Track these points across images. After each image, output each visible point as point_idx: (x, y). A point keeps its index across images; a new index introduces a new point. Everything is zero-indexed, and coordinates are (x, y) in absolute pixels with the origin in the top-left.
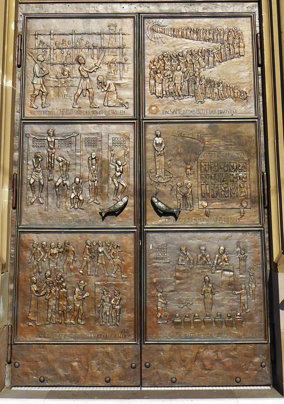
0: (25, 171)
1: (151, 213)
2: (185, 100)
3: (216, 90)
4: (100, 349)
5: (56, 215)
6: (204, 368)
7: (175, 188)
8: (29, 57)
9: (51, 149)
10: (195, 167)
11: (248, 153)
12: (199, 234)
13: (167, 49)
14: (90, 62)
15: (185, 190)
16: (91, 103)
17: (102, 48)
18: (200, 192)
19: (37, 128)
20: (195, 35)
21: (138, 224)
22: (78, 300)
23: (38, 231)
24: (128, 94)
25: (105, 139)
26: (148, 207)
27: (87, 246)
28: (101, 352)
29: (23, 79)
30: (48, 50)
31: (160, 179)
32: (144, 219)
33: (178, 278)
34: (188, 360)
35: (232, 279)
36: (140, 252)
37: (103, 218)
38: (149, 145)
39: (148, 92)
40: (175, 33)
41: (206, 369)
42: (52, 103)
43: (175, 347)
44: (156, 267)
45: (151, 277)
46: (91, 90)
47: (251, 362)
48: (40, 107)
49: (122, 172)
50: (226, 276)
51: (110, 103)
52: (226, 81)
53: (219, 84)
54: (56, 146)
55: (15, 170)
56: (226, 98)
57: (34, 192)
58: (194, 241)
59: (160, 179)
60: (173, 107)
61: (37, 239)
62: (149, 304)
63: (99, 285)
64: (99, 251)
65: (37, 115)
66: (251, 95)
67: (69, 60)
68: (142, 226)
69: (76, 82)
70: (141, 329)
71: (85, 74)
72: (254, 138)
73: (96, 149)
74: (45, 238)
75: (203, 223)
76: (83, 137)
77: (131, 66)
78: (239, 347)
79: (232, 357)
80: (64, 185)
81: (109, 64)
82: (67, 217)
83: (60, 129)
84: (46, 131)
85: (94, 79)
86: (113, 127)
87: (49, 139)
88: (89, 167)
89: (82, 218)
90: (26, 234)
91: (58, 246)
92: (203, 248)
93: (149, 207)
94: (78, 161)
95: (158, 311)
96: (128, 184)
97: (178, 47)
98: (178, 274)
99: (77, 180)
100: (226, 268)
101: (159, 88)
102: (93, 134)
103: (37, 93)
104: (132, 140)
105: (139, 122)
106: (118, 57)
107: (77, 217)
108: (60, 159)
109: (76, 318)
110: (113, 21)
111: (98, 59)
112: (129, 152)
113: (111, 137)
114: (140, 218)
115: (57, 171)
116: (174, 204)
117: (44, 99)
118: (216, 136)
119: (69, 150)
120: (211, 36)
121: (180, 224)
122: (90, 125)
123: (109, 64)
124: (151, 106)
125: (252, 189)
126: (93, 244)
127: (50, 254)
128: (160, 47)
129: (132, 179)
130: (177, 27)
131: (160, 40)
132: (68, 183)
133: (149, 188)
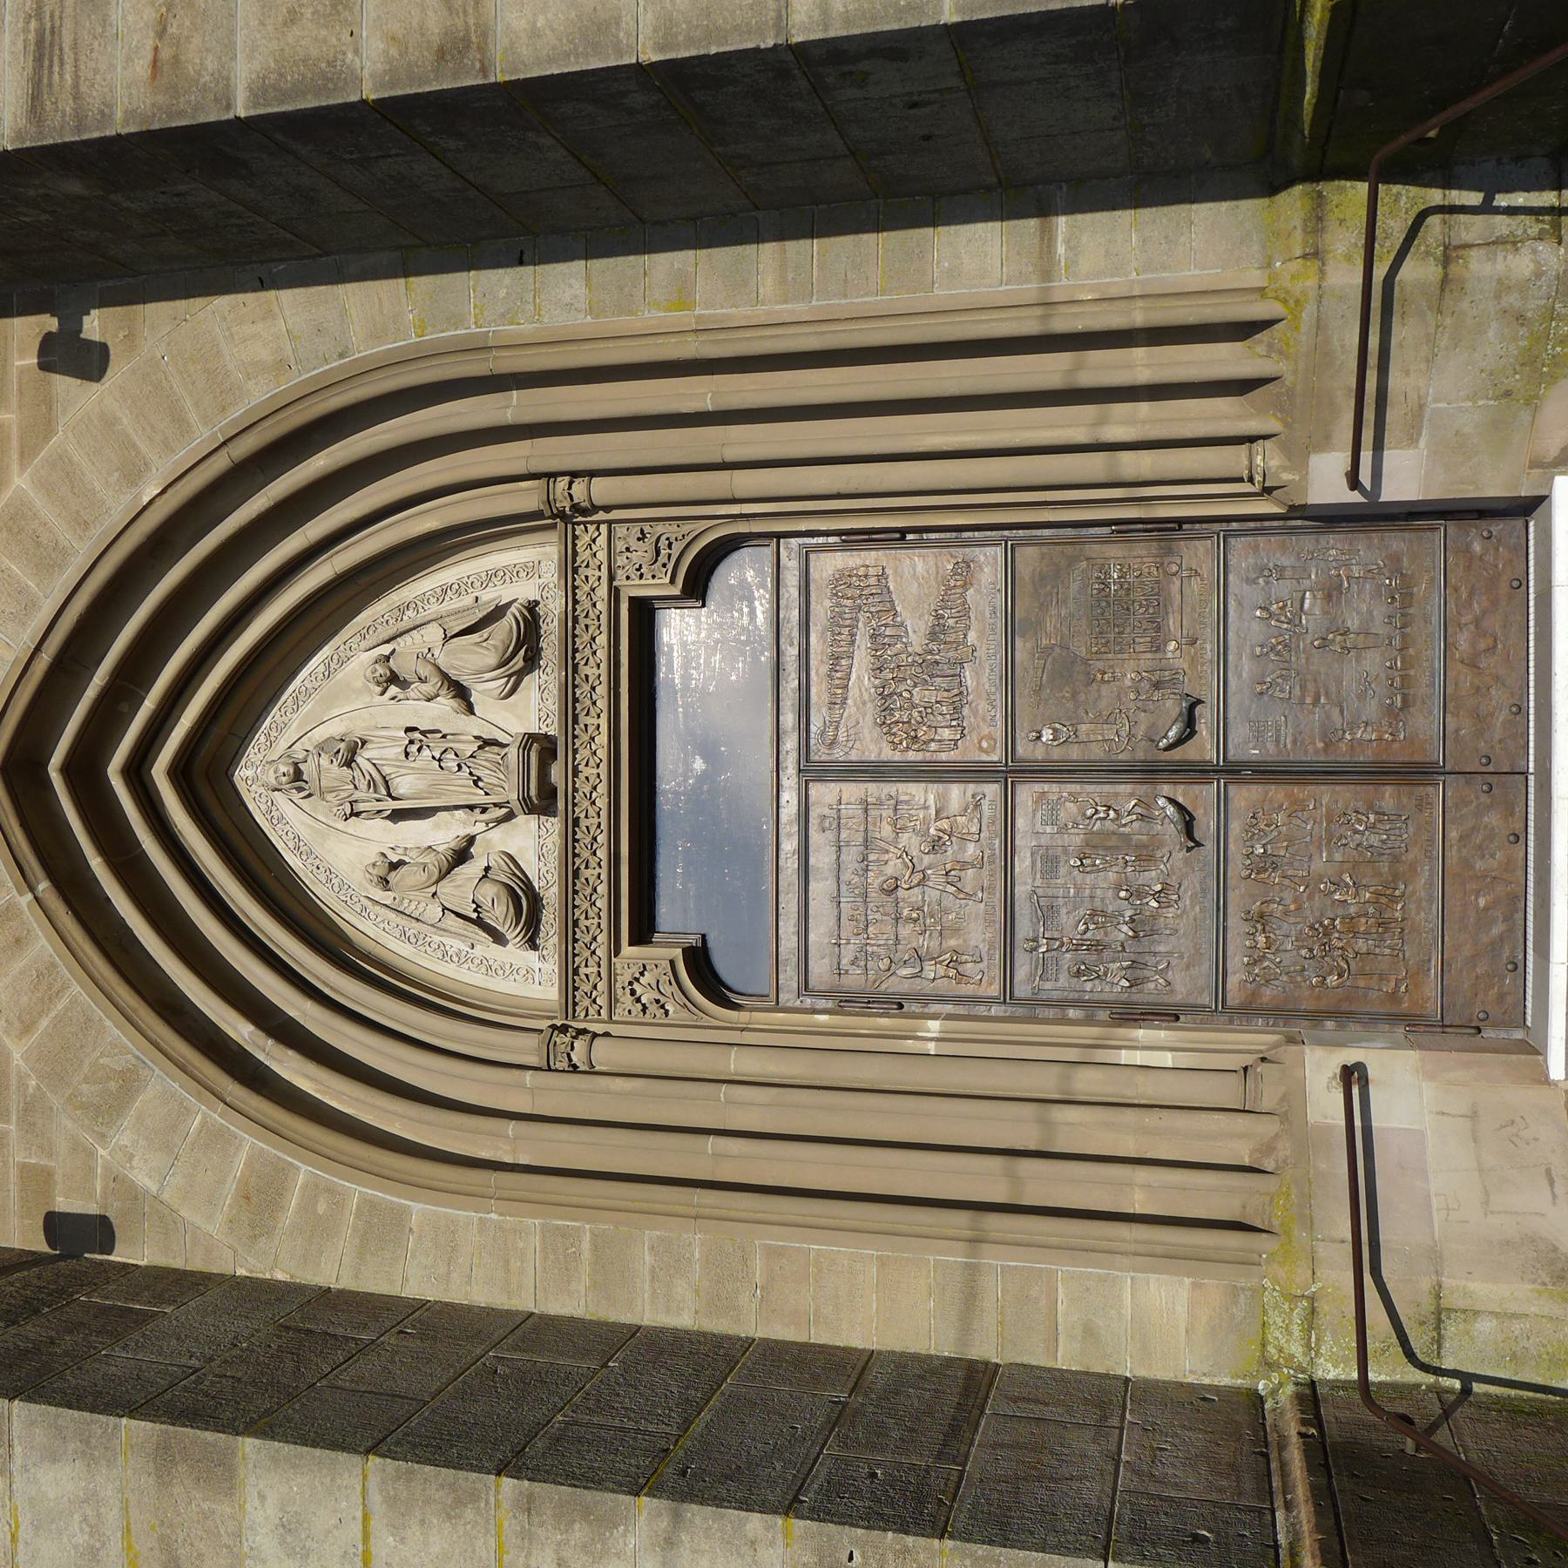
0: (1105, 997)
1: (1189, 752)
2: (969, 683)
3: (951, 622)
4: (1453, 854)
6: (1491, 649)
7: (1140, 704)
8: (883, 987)
9: (1062, 945)
10: (1100, 665)
12: (1230, 658)
13: (869, 718)
14: (893, 867)
15: (1145, 685)
16: (974, 866)
17: (866, 843)
18: (1149, 656)
19: (1021, 973)
20: (843, 662)
22: (1357, 894)
24: (957, 794)
25: (1044, 841)
26: (1177, 758)
28: (1459, 850)
29: (924, 999)
30: (870, 949)
31: (1123, 734)
33: (1317, 700)
34: (1476, 681)
35: (1319, 595)
36: (1265, 772)
37: (1198, 844)
38: (1056, 754)
39: (953, 755)
40: (837, 702)
41: (1495, 647)
42: (972, 943)
43: (1450, 706)
44: (1294, 742)
45: (1313, 752)
46: (948, 867)
47: (1481, 558)
48: (981, 966)
49: (1109, 808)
50: (1312, 605)
51: (974, 829)
52: (933, 602)
53: (938, 617)
55: (1103, 1015)
56: (965, 602)
57: (1146, 980)
58: (1243, 669)
59: (1123, 734)
60: (983, 706)
62: (1366, 756)
63: (1329, 854)
65: (997, 972)
66: (960, 553)
67: (890, 909)
69: (932, 895)
70: (1416, 773)
71: (917, 878)
72: (1045, 549)
73: (1063, 858)
75: (1209, 650)
76: (1038, 883)
77: (901, 787)
78: (1452, 580)
79: (1471, 595)
80: (1132, 920)
81: (898, 830)
83: (1024, 928)
84: (1027, 956)
85: (927, 859)
87: (1044, 949)
88: (1099, 871)
92: (1258, 649)
93: (1177, 754)
94: (1087, 892)
95: (1380, 739)
96: (1132, 795)
97: (866, 697)
98: (1309, 700)
99: (1123, 894)
101: (946, 734)
102: (1033, 863)
103: (952, 973)
104: (1046, 787)
105: (1012, 773)
106: (885, 814)
108: (1082, 927)
109: (1393, 899)
110: (813, 821)
111: (887, 852)
112: (1070, 794)
113: (1039, 828)
114: (1199, 772)
115: (1106, 934)
116: (1173, 706)
117: (964, 958)
118: (1040, 623)
119: (1064, 911)
120: (846, 631)
121: (1210, 695)
122: (1017, 870)
123: (898, 830)
124: (981, 748)
125: (1144, 553)
128: (866, 731)
129: (1121, 788)
130: (826, 697)
131: (851, 732)
132: (1128, 913)
133: (1140, 755)
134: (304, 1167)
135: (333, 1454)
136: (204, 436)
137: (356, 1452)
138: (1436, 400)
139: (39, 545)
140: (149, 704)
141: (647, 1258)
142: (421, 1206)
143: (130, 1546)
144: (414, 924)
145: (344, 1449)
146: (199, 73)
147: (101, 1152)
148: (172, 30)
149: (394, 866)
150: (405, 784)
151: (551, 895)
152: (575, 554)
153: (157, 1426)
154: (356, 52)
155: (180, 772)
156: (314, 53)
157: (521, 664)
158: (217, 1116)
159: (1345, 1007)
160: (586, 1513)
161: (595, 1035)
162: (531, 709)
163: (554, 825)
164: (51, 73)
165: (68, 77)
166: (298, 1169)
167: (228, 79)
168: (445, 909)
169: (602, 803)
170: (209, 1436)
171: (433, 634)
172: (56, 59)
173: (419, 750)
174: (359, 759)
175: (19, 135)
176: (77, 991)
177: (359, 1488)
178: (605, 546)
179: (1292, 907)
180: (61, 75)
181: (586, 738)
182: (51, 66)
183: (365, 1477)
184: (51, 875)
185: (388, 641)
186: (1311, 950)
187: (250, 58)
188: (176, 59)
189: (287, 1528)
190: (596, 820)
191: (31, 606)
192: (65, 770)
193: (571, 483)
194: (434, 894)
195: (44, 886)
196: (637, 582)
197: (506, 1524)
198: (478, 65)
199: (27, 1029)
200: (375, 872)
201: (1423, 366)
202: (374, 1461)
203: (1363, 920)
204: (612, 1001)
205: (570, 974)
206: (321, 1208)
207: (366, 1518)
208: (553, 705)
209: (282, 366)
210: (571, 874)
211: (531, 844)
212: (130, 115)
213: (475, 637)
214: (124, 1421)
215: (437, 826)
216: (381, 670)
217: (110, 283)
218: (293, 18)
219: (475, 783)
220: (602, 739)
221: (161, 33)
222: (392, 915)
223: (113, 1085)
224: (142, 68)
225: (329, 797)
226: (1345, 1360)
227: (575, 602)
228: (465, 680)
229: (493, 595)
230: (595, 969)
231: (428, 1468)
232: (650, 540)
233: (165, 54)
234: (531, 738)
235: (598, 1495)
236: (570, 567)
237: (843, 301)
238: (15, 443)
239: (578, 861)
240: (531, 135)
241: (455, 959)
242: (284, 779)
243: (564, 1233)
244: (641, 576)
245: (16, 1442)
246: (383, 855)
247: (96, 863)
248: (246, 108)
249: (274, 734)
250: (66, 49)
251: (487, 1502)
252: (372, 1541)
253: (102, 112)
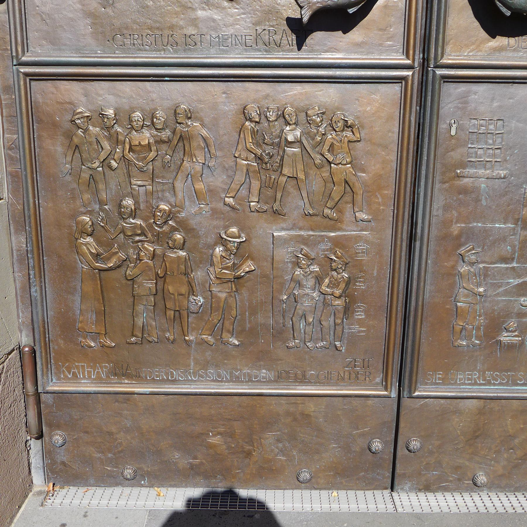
5: (142, 20)
21: (417, 52)
23: (84, 75)
27: (247, 123)
32: (441, 36)
61: (83, 99)
64: (286, 139)
68: (428, 60)
74: (111, 98)
82: (181, 28)
89: (231, 31)
90: (49, 84)
91: (153, 123)
107: (215, 29)
126: (266, 117)
127: (131, 146)
159: (49, 264)
179: (200, 186)
186: (133, 214)
203: (184, 289)
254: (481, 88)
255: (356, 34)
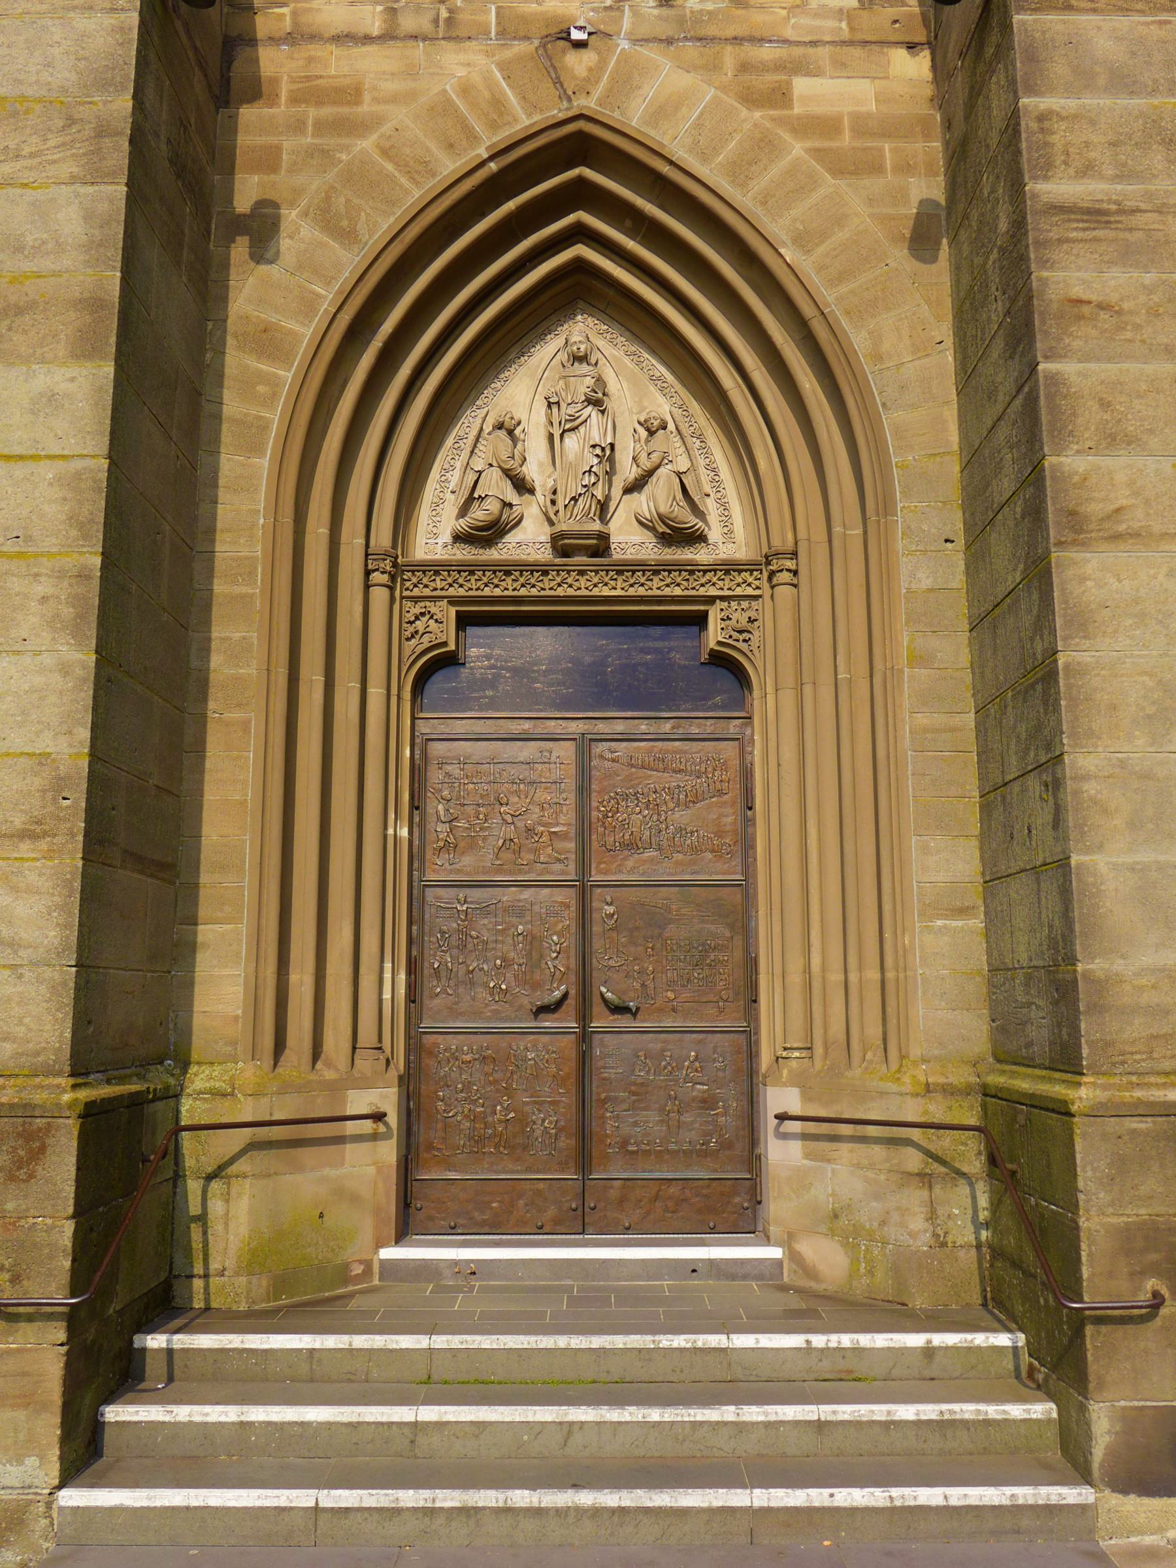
6: (666, 1209)
10: (658, 946)
11: (731, 927)
12: (662, 1035)
19: (441, 892)
26: (594, 999)
28: (531, 1190)
29: (422, 825)
33: (634, 1094)
35: (706, 1095)
36: (584, 1059)
38: (596, 916)
39: (595, 845)
41: (669, 1212)
44: (604, 1079)
45: (596, 1090)
50: (699, 1090)
51: (542, 859)
54: (469, 917)
57: (439, 978)
70: (584, 1160)
73: (524, 920)
75: (668, 1023)
78: (715, 1183)
79: (705, 1196)
83: (476, 894)
86: (546, 891)
92: (669, 1054)
95: (607, 1136)
98: (633, 1088)
99: (498, 962)
100: (699, 1080)
102: (519, 901)
109: (496, 1146)
110: (550, 744)
115: (471, 951)
124: (600, 863)
129: (573, 962)
132: (486, 967)
134: (290, 375)
135: (107, 433)
136: (829, 296)
137: (110, 449)
138: (833, 1171)
139: (750, 164)
140: (631, 245)
141: (238, 635)
142: (266, 465)
143: (27, 277)
144: (469, 449)
145: (111, 440)
146: (1071, 334)
147: (294, 213)
148: (1104, 315)
149: (511, 432)
150: (572, 443)
151: (493, 554)
152: (740, 571)
153: (117, 300)
154: (1078, 452)
155: (579, 266)
156: (1080, 421)
157: (661, 530)
158: (326, 306)
160: (81, 616)
161: (392, 589)
162: (629, 538)
163: (544, 555)
164: (1078, 221)
165: (1074, 234)
166: (289, 371)
167: (1065, 356)
168: (480, 472)
169: (560, 592)
170: (113, 340)
171: (683, 464)
172: (1086, 225)
173: (597, 455)
174: (590, 408)
175: (1035, 196)
176: (416, 195)
177: (85, 452)
178: (745, 593)
180: (1076, 229)
181: (606, 579)
182: (1083, 221)
183: (93, 457)
184: (503, 171)
185: (677, 428)
186: (462, 1091)
187: (1080, 374)
188: (1080, 317)
189: (52, 398)
190: (547, 587)
191: (705, 158)
192: (581, 181)
193: (789, 570)
194: (491, 465)
195: (493, 166)
196: (719, 617)
197: (69, 560)
198: (1063, 539)
199: (385, 152)
200: (507, 419)
201: (855, 1162)
202: (105, 463)
204: (416, 600)
205: (435, 568)
206: (261, 389)
207: (63, 457)
208: (630, 555)
209: (878, 357)
210: (507, 569)
211: (530, 539)
212: (1044, 282)
213: (679, 496)
214: (119, 274)
215: (541, 465)
216: (656, 423)
217: (943, 223)
218: (1105, 405)
219: (573, 498)
220: (606, 592)
221: (1101, 306)
222: (474, 432)
223: (345, 223)
224: (1077, 292)
225: (561, 383)
226: (192, 1117)
227: (705, 572)
228: (647, 489)
229: (711, 507)
230: (439, 587)
231: (103, 503)
232: (749, 627)
233: (1086, 310)
234: (604, 538)
235: (94, 625)
236: (729, 568)
237: (910, 773)
238: (826, 144)
239: (517, 574)
240: (1021, 566)
241: (443, 478)
242: (575, 348)
243: (252, 573)
244: (722, 619)
245: (96, 188)
246: (519, 423)
247: (511, 205)
248: (1044, 370)
249: (609, 336)
250: (1095, 233)
251: (83, 546)
252: (48, 462)
253: (1047, 261)
254: (608, 1036)
255: (556, 1015)
